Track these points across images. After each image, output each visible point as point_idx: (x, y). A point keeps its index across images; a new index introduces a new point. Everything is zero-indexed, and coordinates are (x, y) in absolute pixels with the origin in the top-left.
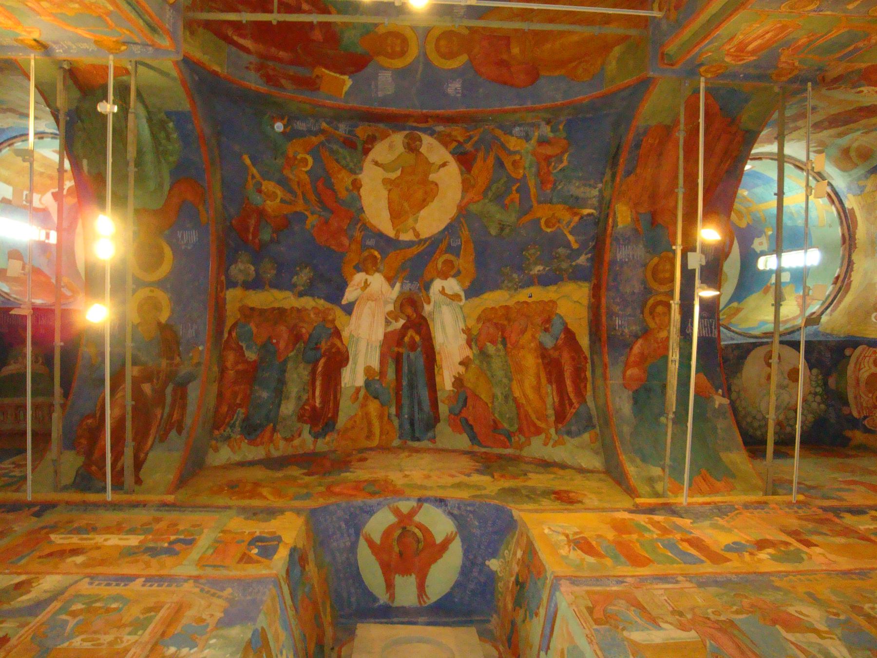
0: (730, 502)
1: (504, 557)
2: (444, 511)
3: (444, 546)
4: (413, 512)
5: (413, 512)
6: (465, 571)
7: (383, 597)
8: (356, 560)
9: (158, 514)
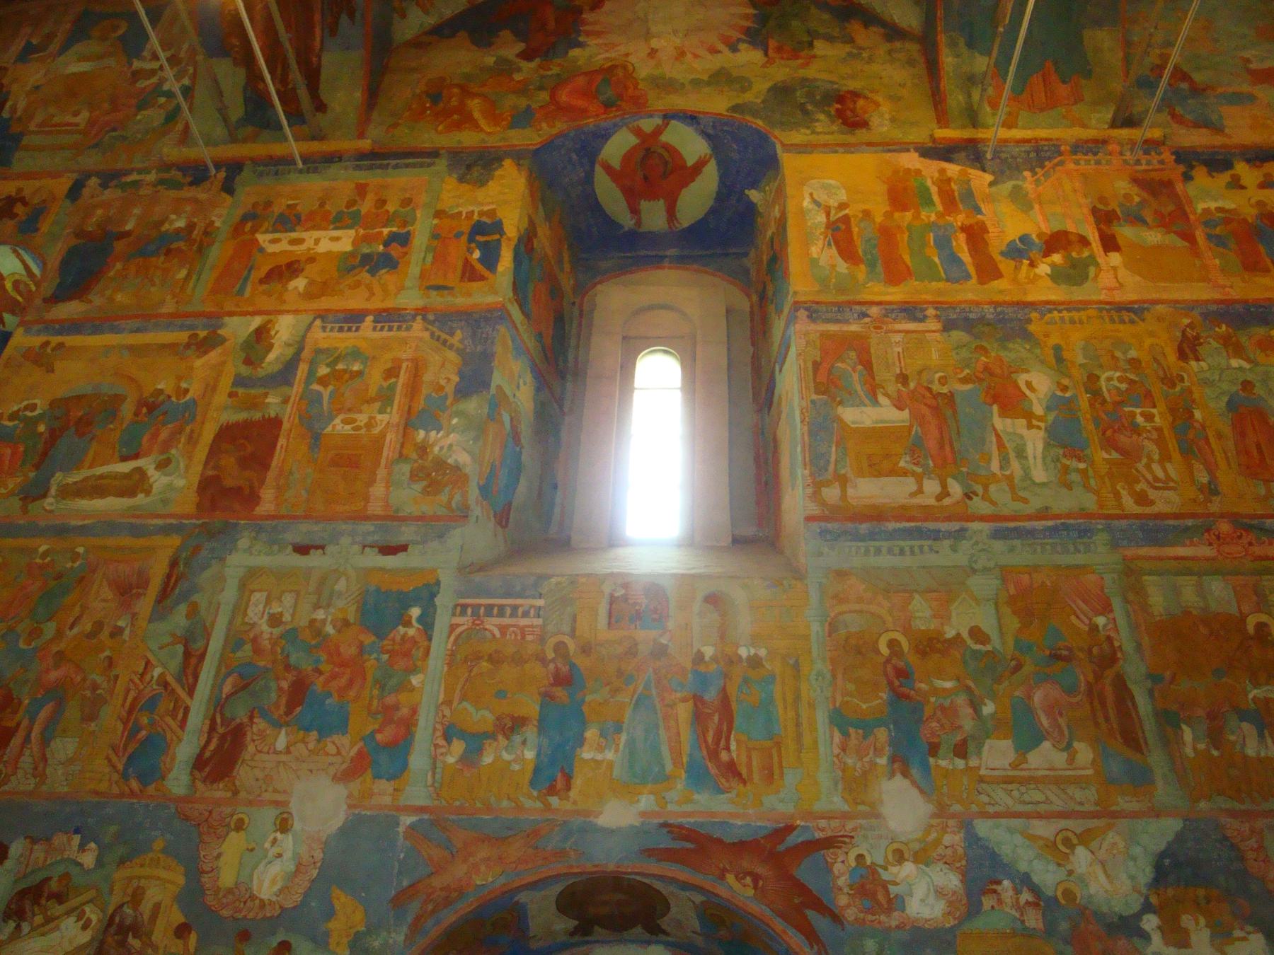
0: (1057, 139)
1: (765, 192)
2: (696, 130)
4: (658, 131)
5: (658, 131)
7: (627, 221)
8: (593, 190)
9: (362, 177)
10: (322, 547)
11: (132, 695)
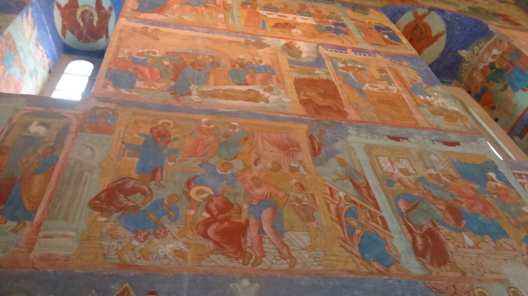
1: (473, 51)
2: (442, 17)
3: (436, 38)
4: (424, 16)
5: (424, 16)
6: (443, 54)
10: (407, 139)
11: (333, 208)
